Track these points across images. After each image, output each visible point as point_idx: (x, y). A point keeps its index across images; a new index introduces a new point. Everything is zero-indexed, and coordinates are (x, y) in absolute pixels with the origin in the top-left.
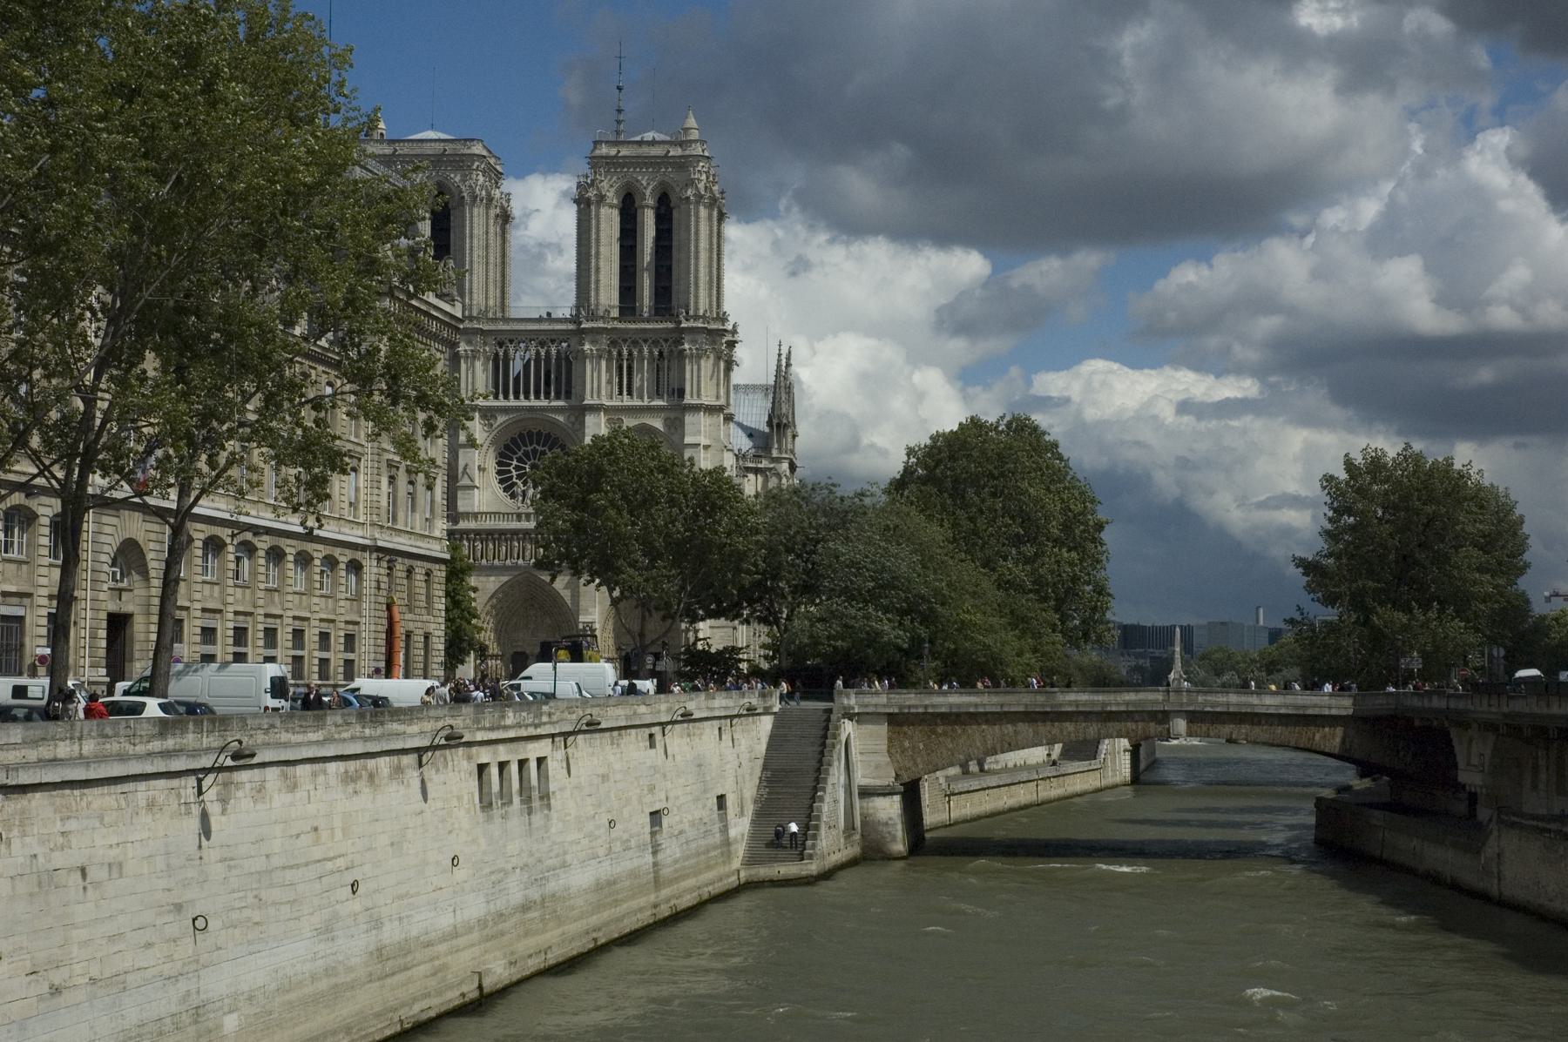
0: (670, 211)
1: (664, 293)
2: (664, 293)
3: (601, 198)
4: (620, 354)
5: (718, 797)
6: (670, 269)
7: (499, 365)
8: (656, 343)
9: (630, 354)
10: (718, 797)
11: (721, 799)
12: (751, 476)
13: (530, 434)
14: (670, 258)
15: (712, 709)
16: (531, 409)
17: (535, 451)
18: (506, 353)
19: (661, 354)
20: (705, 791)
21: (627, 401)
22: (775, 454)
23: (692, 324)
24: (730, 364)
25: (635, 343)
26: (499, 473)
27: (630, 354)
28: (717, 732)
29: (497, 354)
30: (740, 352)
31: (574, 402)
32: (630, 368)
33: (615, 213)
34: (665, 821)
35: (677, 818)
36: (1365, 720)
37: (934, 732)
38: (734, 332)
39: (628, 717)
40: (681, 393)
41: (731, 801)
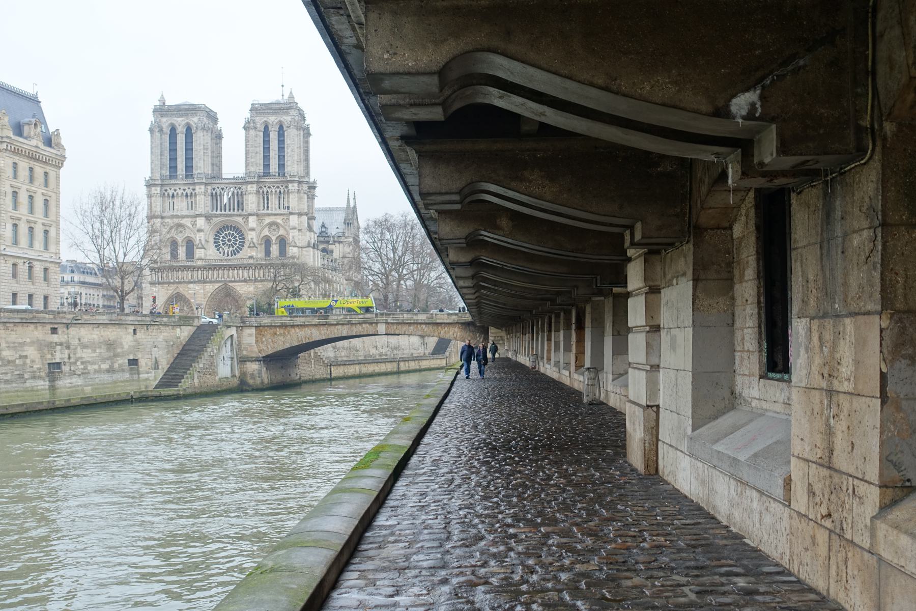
0: (284, 132)
1: (281, 166)
2: (281, 166)
3: (255, 128)
4: (263, 192)
5: (129, 360)
6: (284, 156)
7: (215, 197)
8: (278, 187)
9: (267, 192)
10: (129, 360)
11: (134, 362)
12: (337, 244)
13: (227, 226)
14: (284, 152)
15: (125, 320)
16: (227, 216)
17: (229, 233)
18: (216, 193)
19: (280, 192)
20: (116, 355)
21: (266, 211)
22: (346, 235)
23: (292, 179)
24: (311, 198)
25: (269, 187)
26: (215, 243)
27: (267, 192)
28: (132, 331)
29: (212, 193)
30: (317, 191)
31: (244, 212)
32: (268, 198)
33: (261, 134)
34: (65, 368)
35: (82, 367)
36: (463, 324)
37: (276, 334)
38: (315, 182)
39: (22, 319)
40: (288, 208)
41: (142, 362)
